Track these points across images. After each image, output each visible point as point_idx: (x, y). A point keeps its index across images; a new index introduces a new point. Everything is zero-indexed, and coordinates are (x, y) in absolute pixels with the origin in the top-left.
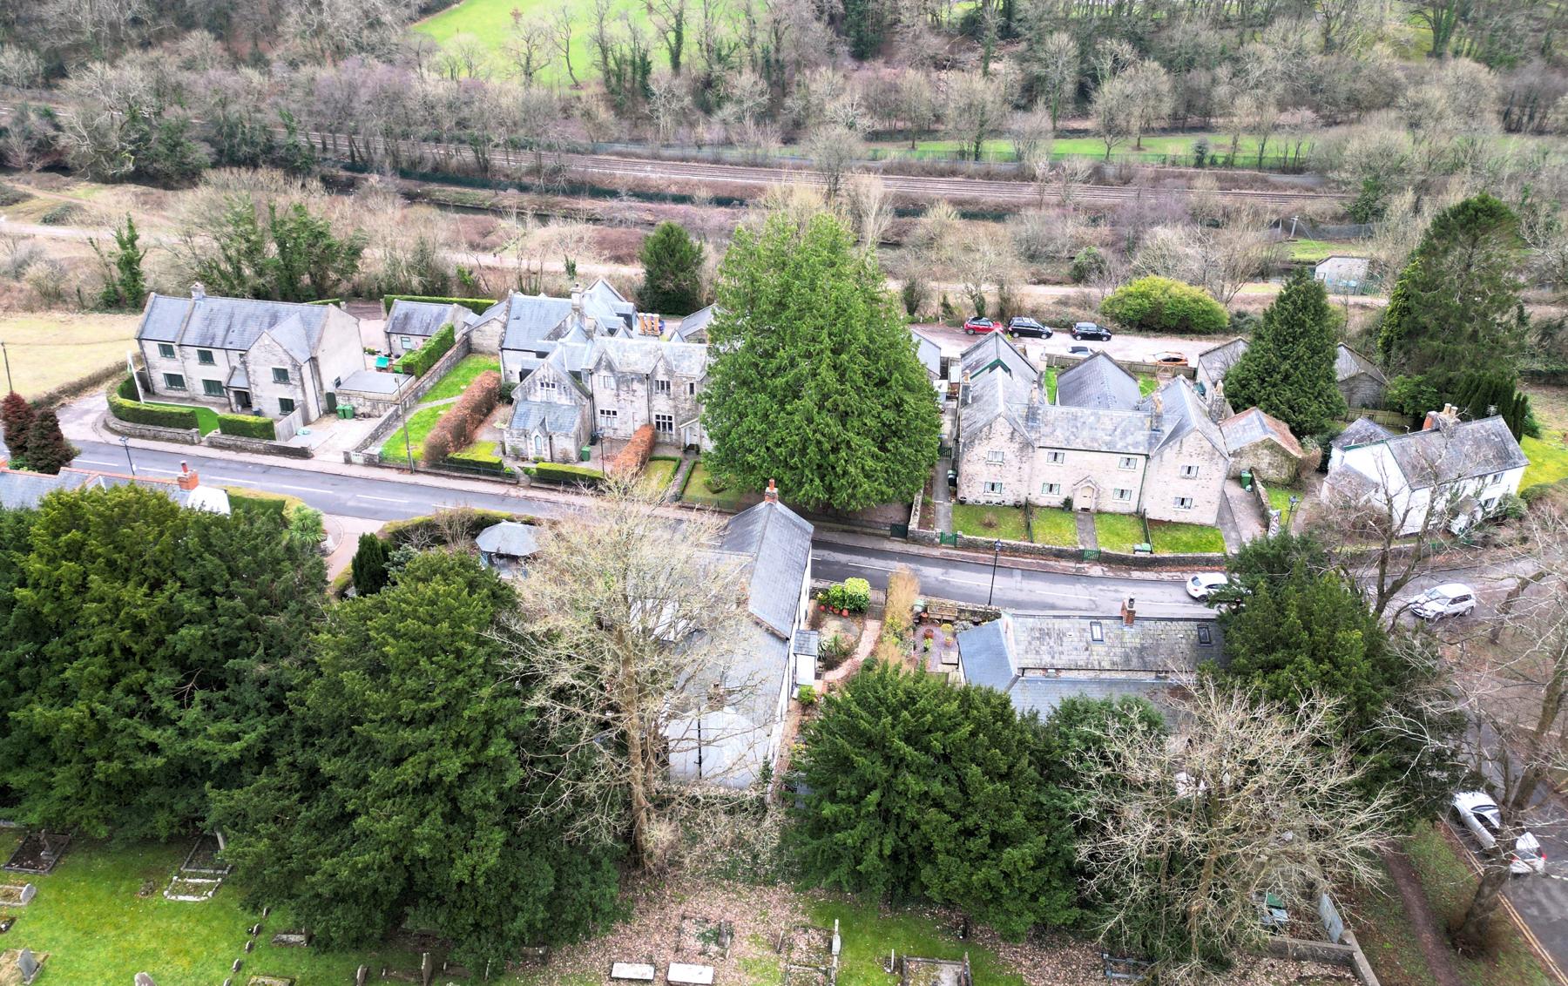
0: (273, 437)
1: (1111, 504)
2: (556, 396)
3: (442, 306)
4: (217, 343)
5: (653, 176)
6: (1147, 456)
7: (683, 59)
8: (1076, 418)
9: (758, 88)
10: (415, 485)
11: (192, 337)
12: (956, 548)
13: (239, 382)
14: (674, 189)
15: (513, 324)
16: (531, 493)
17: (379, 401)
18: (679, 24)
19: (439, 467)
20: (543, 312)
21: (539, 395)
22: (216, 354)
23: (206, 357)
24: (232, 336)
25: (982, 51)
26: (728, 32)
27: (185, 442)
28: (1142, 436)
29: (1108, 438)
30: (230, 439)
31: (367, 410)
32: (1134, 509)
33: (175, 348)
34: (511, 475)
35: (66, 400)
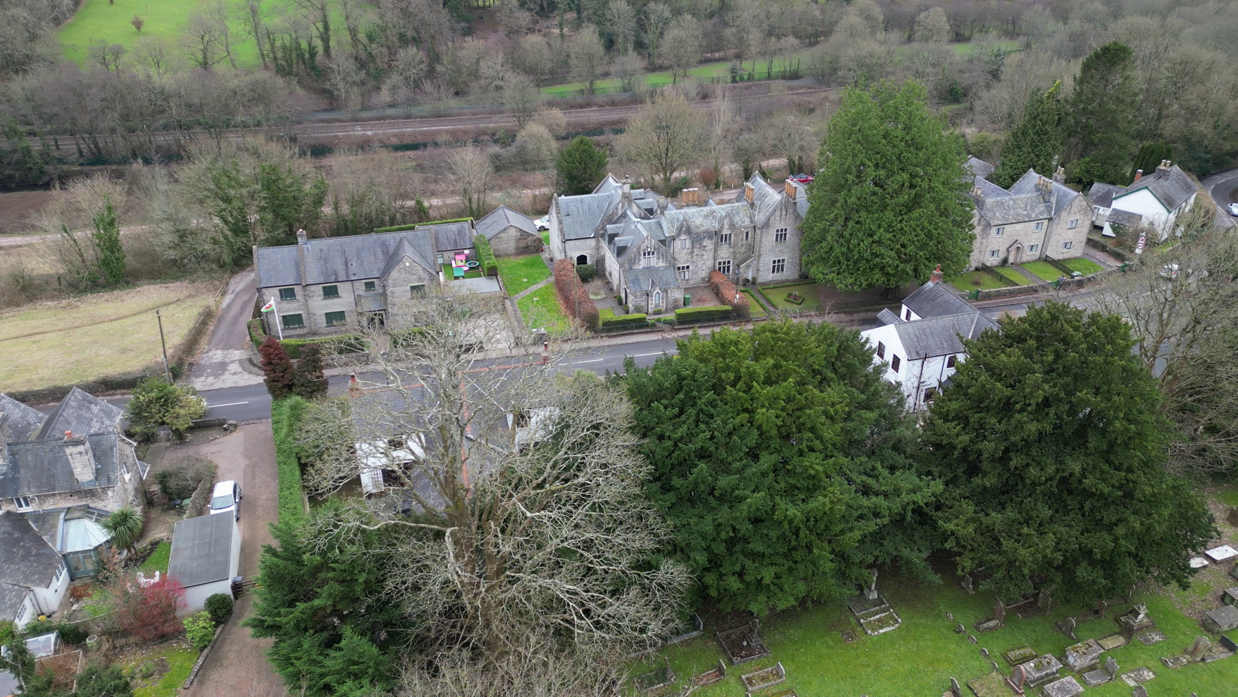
1: (1028, 256)
2: (654, 261)
3: (458, 225)
4: (342, 277)
5: (370, 133)
6: (1050, 219)
7: (332, 43)
8: (1003, 204)
11: (313, 273)
12: (977, 300)
14: (395, 141)
15: (567, 221)
18: (325, 16)
21: (643, 263)
22: (343, 288)
24: (354, 267)
25: (558, 18)
26: (367, 19)
28: (1041, 207)
32: (1036, 254)
33: (297, 289)
34: (654, 325)
35: (190, 360)
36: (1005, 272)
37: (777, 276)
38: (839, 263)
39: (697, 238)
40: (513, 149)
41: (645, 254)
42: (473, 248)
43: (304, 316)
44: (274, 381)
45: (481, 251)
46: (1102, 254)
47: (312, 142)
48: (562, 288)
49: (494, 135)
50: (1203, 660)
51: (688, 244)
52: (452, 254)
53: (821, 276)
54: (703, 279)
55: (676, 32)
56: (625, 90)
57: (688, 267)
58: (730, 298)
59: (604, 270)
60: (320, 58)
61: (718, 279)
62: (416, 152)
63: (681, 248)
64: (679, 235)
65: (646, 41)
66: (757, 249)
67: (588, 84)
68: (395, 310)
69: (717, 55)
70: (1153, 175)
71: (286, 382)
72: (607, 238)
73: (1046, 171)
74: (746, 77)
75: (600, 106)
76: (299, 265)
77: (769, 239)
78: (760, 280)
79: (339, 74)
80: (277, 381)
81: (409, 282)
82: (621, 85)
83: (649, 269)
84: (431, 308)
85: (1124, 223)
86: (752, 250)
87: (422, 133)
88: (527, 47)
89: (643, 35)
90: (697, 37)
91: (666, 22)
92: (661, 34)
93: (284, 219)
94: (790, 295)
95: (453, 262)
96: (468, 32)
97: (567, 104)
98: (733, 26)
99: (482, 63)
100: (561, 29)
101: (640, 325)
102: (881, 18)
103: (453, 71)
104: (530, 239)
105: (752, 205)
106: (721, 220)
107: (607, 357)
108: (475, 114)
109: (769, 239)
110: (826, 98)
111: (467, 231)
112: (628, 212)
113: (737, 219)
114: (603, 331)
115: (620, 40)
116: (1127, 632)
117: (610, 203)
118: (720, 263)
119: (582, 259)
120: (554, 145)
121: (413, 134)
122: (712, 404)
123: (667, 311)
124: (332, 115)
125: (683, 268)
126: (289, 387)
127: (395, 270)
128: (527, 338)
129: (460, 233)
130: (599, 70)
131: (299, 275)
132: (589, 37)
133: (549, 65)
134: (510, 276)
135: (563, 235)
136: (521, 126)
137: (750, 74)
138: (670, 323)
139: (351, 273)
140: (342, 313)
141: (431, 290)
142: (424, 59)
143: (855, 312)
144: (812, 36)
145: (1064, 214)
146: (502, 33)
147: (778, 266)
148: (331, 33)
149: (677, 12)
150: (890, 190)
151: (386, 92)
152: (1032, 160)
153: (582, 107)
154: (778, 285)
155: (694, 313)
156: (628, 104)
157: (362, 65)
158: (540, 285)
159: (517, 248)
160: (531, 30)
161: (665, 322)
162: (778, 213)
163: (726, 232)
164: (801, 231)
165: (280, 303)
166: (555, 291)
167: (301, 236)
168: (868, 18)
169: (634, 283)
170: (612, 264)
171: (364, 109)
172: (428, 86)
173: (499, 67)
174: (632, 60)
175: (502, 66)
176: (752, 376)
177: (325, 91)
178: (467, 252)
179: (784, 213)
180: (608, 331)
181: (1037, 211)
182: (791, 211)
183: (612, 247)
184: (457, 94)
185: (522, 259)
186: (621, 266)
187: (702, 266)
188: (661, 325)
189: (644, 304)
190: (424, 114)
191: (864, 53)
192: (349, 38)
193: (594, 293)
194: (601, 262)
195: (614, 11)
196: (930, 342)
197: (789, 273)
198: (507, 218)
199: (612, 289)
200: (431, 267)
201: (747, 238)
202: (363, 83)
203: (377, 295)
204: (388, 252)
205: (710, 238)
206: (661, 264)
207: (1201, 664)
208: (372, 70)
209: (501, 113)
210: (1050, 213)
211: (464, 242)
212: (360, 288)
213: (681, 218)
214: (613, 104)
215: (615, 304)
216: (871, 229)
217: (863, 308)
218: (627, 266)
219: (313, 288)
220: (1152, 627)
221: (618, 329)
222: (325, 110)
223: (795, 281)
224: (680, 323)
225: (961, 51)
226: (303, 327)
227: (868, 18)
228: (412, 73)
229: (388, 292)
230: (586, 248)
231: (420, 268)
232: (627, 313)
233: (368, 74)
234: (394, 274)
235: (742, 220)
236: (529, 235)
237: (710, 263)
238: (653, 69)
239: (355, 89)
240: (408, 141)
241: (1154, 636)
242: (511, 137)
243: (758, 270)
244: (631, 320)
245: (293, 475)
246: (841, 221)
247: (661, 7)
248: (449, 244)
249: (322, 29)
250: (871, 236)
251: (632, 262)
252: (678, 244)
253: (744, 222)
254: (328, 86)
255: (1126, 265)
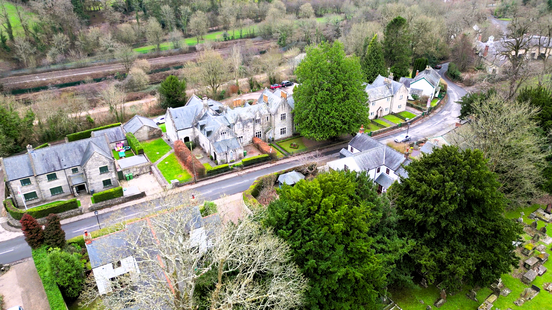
0: (122, 195)
1: (385, 113)
3: (115, 128)
4: (58, 167)
5: (44, 79)
7: (14, 34)
8: (373, 92)
9: (65, 39)
10: (203, 186)
11: (40, 168)
13: (77, 181)
14: (59, 82)
15: (176, 121)
16: (247, 171)
17: (143, 167)
18: (8, 20)
19: (203, 177)
20: (185, 113)
21: (221, 138)
23: (52, 177)
24: (64, 162)
27: (77, 215)
29: (382, 95)
30: (99, 204)
31: (137, 173)
34: (232, 169)
36: (378, 121)
37: (283, 136)
38: (315, 128)
39: (245, 123)
40: (126, 81)
41: (221, 134)
42: (126, 139)
43: (37, 193)
44: (31, 239)
45: (132, 141)
46: (412, 108)
47: (12, 87)
48: (180, 155)
49: (113, 74)
50: (530, 299)
51: (241, 126)
52: (114, 144)
53: (308, 135)
54: (250, 142)
55: (196, 19)
56: (176, 48)
57: (242, 137)
58: (266, 150)
59: (199, 143)
60: (8, 42)
61: (257, 141)
62: (72, 87)
63: (238, 129)
64: (236, 122)
65: (181, 24)
66: (273, 124)
67: (156, 46)
68: (92, 182)
69: (214, 28)
70: (424, 72)
71: (39, 238)
72: (199, 127)
73: (385, 75)
74: (231, 38)
75: (164, 56)
76: (30, 165)
77: (277, 120)
78: (276, 139)
79: (21, 50)
80: (34, 239)
81: (98, 165)
82: (173, 45)
83: (224, 141)
84: (113, 176)
85: (416, 94)
86: (270, 126)
87: (74, 77)
88: (123, 30)
89: (179, 21)
90: (205, 21)
91: (190, 14)
92: (188, 20)
93: (12, 136)
94: (291, 144)
95: (116, 148)
96: (89, 24)
97: (148, 56)
98: (221, 15)
99: (100, 39)
100: (138, 21)
101: (226, 170)
102: (285, 8)
103: (85, 44)
104: (155, 131)
105: (268, 104)
106: (255, 113)
107: (214, 190)
108: (101, 65)
109: (277, 120)
110: (270, 46)
111: (121, 131)
112: (208, 113)
113: (261, 111)
114: (208, 176)
115: (169, 24)
116: (497, 292)
117: (197, 110)
118: (256, 133)
119: (187, 139)
120: (147, 77)
121: (69, 78)
122: (309, 224)
123: (236, 160)
124: (20, 72)
125: (240, 138)
126: (42, 241)
127: (90, 160)
128: (169, 186)
129: (117, 132)
130: (161, 39)
131: (32, 170)
132: (153, 24)
133: (135, 38)
134: (149, 152)
135: (176, 128)
136: (128, 70)
137: (232, 37)
138: (240, 166)
139: (62, 165)
140: (61, 186)
141: (111, 168)
142: (68, 39)
143: (322, 149)
144: (258, 18)
145: (397, 93)
146: (107, 23)
147: (283, 131)
148: (12, 29)
149: (194, 10)
150: (334, 93)
151: (50, 57)
152: (375, 70)
153: (155, 57)
154: (284, 140)
155: (251, 160)
156: (178, 54)
157: (33, 43)
158: (167, 155)
159: (149, 136)
160: (122, 22)
161: (238, 166)
162: (281, 107)
163: (258, 118)
164: (293, 114)
165: (21, 188)
166: (176, 157)
167: (29, 148)
168: (280, 8)
169: (218, 149)
170: (204, 140)
171: (38, 66)
172: (73, 53)
173: (109, 41)
174: (176, 33)
175: (111, 40)
176: (327, 206)
177: (14, 59)
178: (123, 142)
179: (284, 106)
180: (210, 175)
181: (387, 93)
182: (286, 105)
183: (203, 131)
184: (89, 55)
185: (153, 142)
186: (210, 141)
187: (248, 136)
188: (236, 168)
189: (225, 158)
190: (73, 67)
191: (283, 25)
192: (23, 30)
193: (197, 154)
194: (197, 139)
195: (163, 10)
196: (369, 162)
197: (288, 134)
198: (141, 122)
199: (205, 152)
200: (109, 156)
201: (268, 120)
202: (35, 53)
203: (80, 174)
204: (83, 151)
205: (251, 122)
206: (230, 137)
207: (529, 301)
208: (39, 46)
209: (115, 63)
210: (391, 93)
211: (121, 137)
212: (70, 172)
213: (236, 114)
214: (171, 55)
215: (210, 161)
216: (328, 111)
217: (326, 147)
218: (213, 141)
219: (41, 177)
220: (503, 286)
221: (214, 174)
222: (16, 69)
223: (291, 137)
224: (245, 166)
225: (320, 21)
226: (38, 198)
227: (280, 8)
228: (63, 46)
229: (87, 173)
230: (188, 133)
231: (104, 157)
232: (217, 164)
233: (37, 48)
234: (89, 162)
235: (264, 111)
236: (154, 129)
237: (252, 134)
238: (187, 36)
239: (32, 57)
240: (66, 82)
241: (506, 291)
242: (122, 76)
243: (274, 134)
244: (222, 168)
245: (58, 297)
246: (314, 109)
247: (186, 7)
248: (112, 139)
249: (7, 27)
250: (328, 114)
251: (216, 138)
252: (236, 125)
253: (265, 112)
254: (15, 57)
255: (424, 113)
